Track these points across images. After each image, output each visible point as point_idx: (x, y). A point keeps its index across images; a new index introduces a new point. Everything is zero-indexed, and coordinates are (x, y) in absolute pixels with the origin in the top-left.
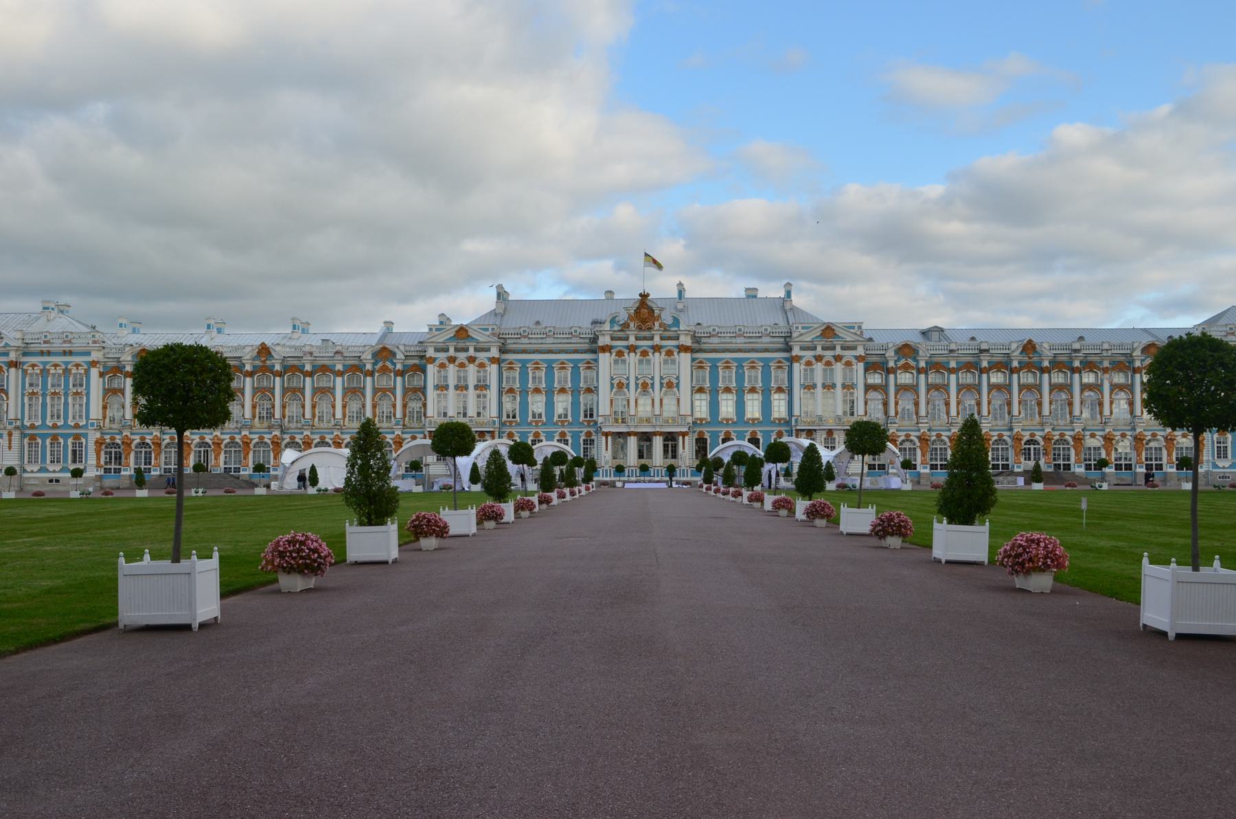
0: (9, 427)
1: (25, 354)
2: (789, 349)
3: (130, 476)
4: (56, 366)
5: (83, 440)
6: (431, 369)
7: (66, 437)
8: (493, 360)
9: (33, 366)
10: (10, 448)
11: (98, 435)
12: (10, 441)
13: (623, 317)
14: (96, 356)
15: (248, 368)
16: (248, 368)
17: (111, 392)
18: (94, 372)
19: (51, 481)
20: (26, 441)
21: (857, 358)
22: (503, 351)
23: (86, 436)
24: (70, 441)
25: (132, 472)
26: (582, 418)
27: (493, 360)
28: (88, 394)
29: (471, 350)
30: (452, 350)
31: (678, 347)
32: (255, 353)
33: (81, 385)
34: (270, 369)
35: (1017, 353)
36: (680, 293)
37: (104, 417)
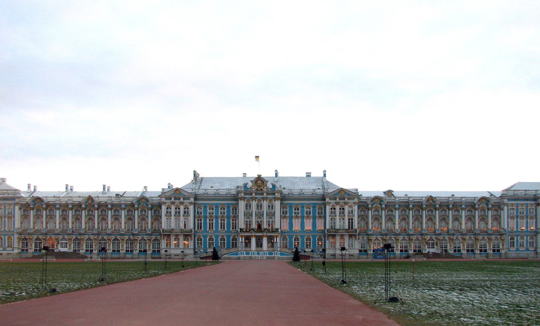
2: (324, 199)
5: (12, 237)
6: (164, 208)
8: (191, 203)
13: (250, 185)
18: (17, 208)
21: (354, 203)
22: (195, 199)
23: (13, 235)
24: (6, 237)
26: (231, 229)
27: (191, 203)
29: (182, 199)
30: (173, 199)
31: (274, 198)
35: (425, 202)
36: (276, 174)
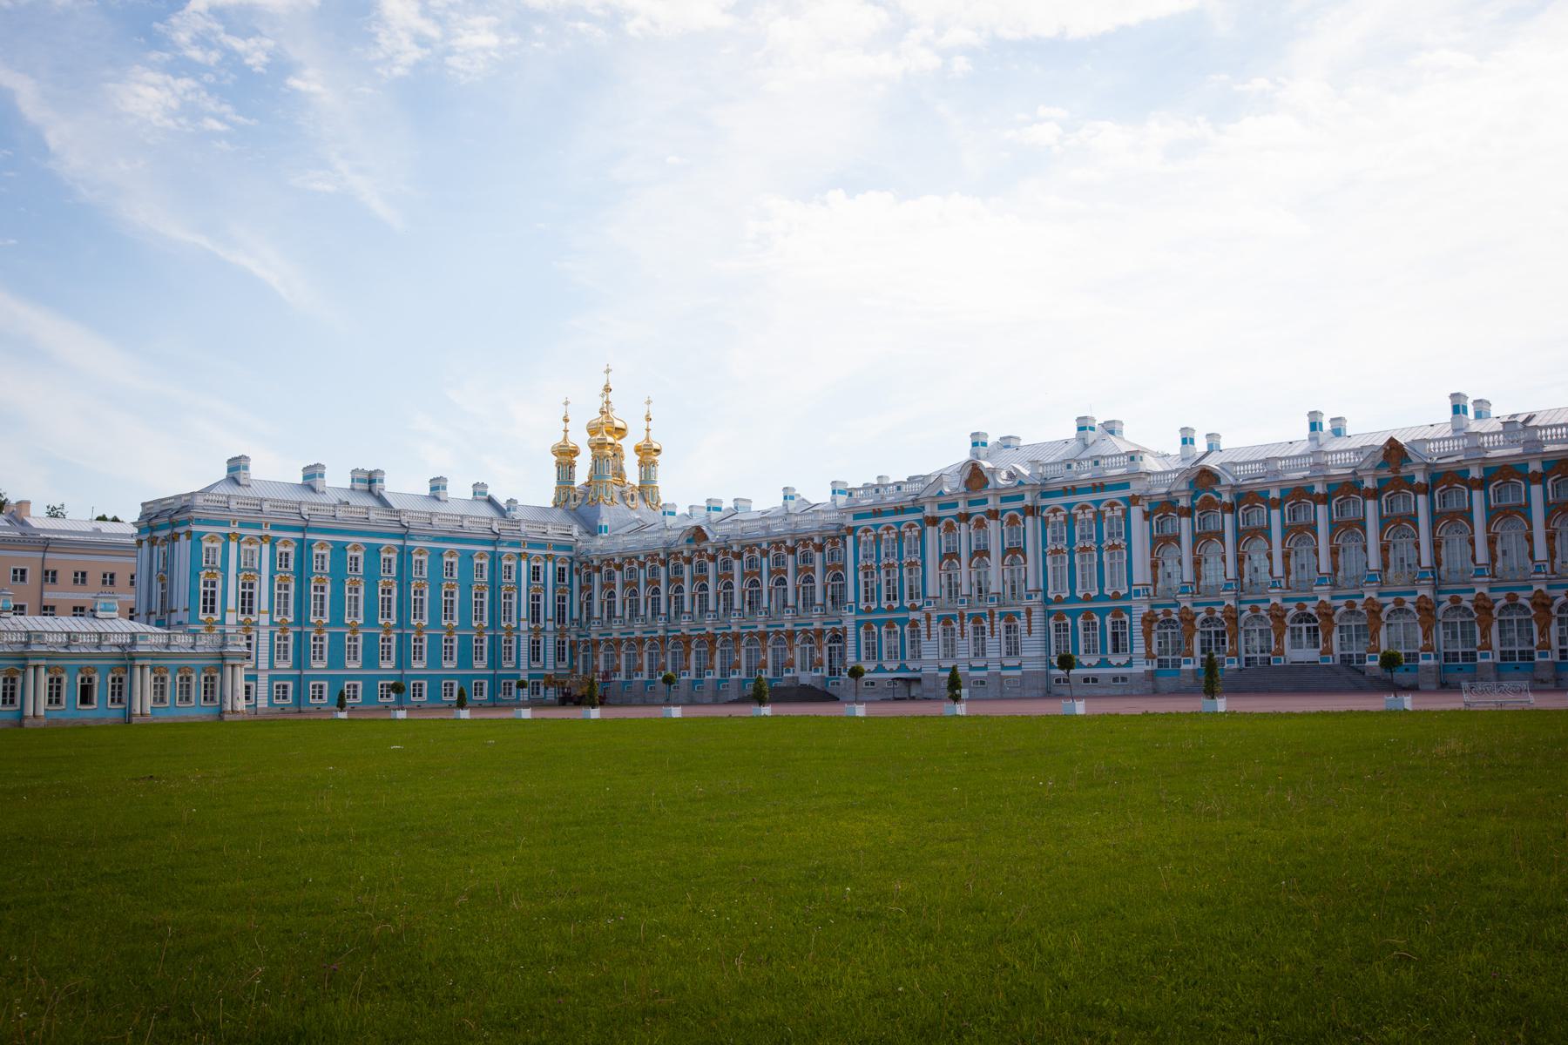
0: (1026, 603)
1: (1044, 495)
3: (1194, 671)
4: (1084, 508)
5: (1126, 618)
7: (1103, 613)
9: (1055, 511)
10: (1030, 632)
11: (1146, 608)
12: (1029, 622)
14: (1136, 488)
15: (1369, 483)
16: (1369, 483)
17: (1163, 541)
18: (1136, 513)
19: (1086, 680)
20: (1052, 622)
23: (1129, 610)
24: (1108, 619)
25: (1198, 665)
28: (1129, 548)
32: (1379, 458)
33: (1119, 534)
34: (1408, 482)
37: (1155, 580)
